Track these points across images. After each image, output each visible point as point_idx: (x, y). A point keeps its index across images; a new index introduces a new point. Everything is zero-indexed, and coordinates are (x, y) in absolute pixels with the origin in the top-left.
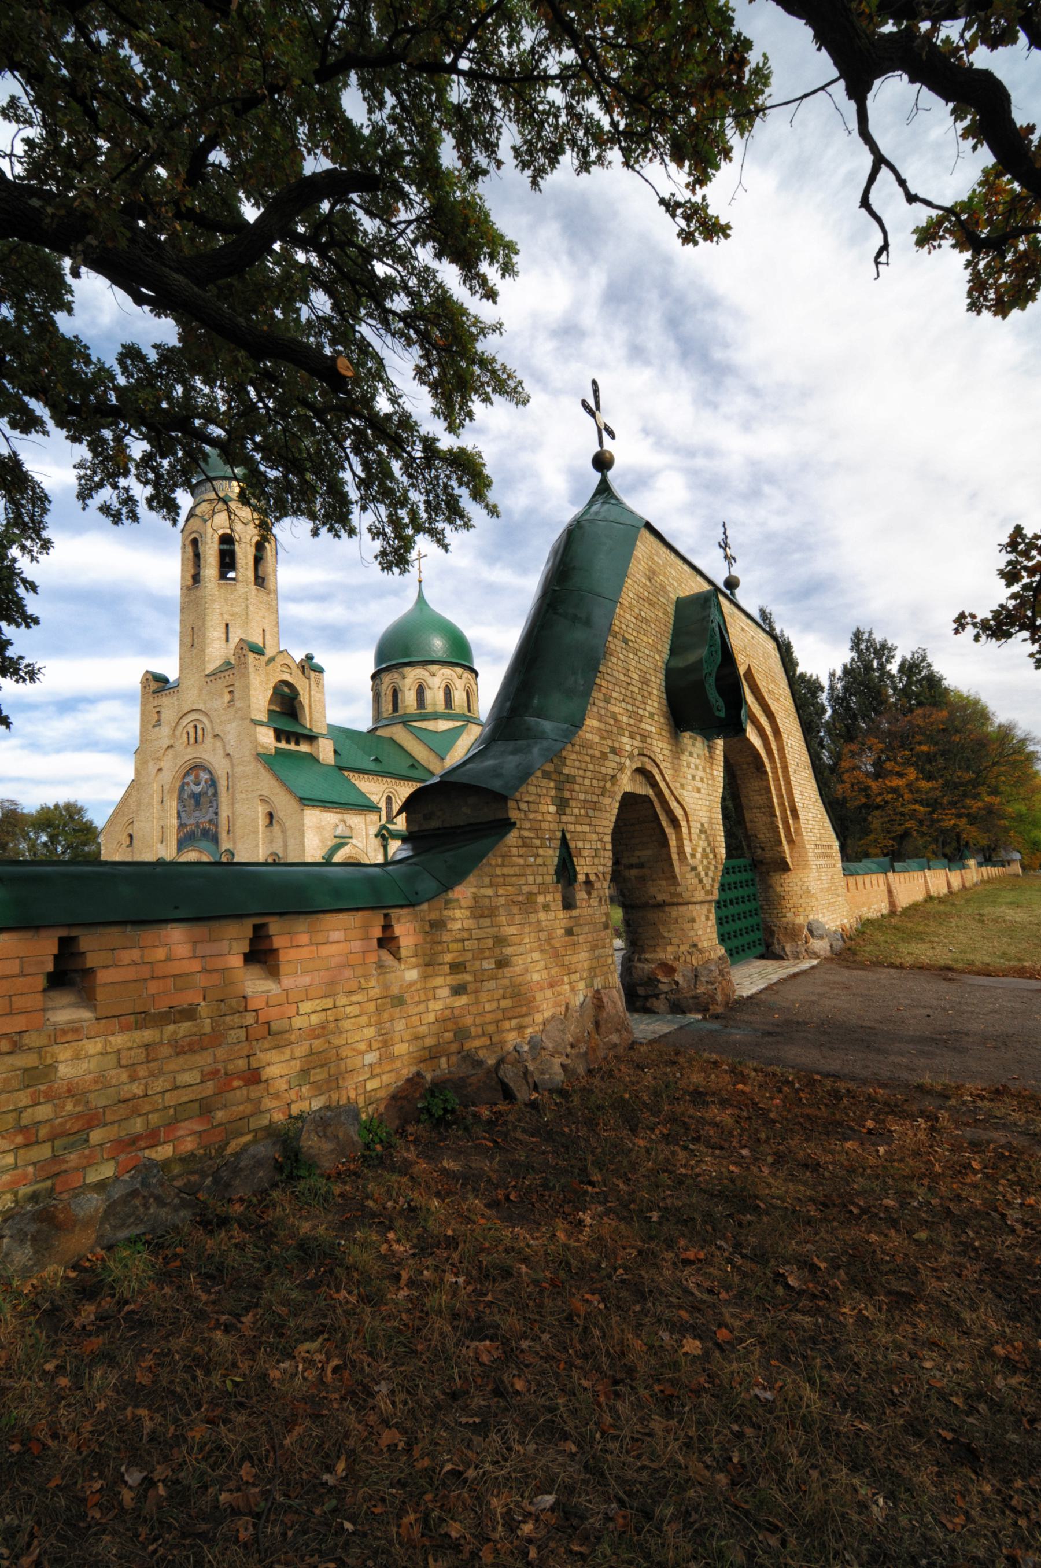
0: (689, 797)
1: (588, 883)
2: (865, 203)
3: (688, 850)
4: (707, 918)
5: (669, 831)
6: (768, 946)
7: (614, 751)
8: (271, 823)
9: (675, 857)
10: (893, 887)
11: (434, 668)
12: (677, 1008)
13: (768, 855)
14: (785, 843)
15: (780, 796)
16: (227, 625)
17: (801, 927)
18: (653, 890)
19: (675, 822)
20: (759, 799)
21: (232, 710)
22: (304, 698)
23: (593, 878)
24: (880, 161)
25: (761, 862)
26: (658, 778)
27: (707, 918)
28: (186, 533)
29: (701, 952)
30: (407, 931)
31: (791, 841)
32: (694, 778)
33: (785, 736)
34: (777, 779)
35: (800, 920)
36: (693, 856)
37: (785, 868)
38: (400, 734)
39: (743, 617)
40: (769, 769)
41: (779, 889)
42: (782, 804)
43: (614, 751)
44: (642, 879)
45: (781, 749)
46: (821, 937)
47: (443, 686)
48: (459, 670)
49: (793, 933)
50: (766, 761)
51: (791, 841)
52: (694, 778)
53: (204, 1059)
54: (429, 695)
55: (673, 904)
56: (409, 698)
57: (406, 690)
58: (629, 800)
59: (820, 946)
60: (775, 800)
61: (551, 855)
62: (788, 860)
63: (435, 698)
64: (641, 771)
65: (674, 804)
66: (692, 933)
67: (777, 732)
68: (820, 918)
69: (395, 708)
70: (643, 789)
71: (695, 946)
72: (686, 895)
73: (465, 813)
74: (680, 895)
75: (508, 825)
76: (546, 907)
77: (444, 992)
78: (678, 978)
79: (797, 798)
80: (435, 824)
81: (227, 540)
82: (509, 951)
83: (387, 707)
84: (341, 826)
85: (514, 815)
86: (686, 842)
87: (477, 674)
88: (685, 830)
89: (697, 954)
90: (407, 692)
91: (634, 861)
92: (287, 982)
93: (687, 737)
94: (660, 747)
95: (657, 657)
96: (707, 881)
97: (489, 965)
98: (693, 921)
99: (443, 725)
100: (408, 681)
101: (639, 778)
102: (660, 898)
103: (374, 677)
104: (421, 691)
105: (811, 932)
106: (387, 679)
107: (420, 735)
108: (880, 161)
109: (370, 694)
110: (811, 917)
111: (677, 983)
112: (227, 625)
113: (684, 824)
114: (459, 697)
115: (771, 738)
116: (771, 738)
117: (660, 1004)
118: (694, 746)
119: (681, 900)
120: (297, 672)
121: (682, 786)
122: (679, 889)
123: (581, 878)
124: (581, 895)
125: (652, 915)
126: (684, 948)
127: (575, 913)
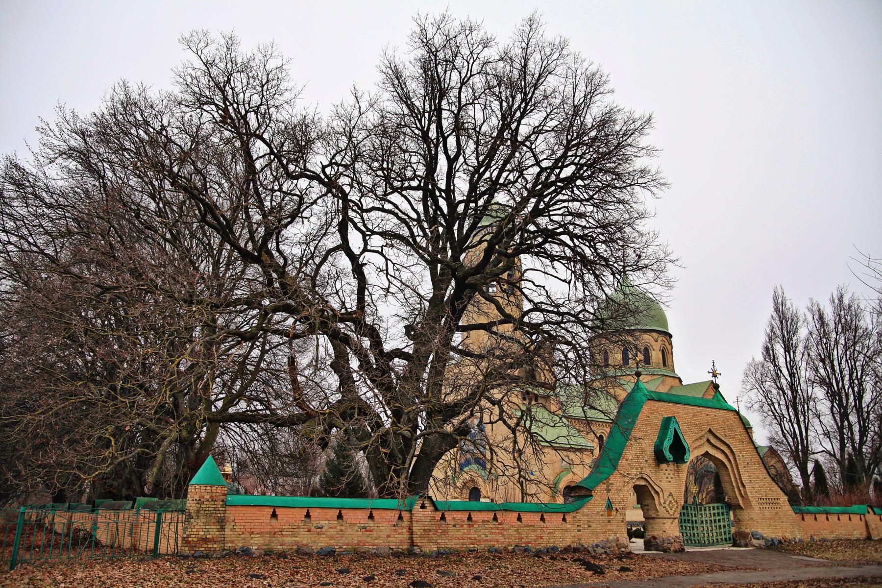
1: (617, 510)
3: (662, 501)
5: (655, 495)
14: (739, 498)
17: (748, 534)
19: (657, 492)
20: (726, 478)
30: (569, 518)
33: (737, 454)
34: (733, 471)
42: (736, 481)
45: (735, 459)
46: (758, 539)
48: (655, 335)
51: (742, 497)
60: (733, 479)
61: (605, 503)
62: (742, 505)
65: (656, 487)
73: (583, 493)
87: (671, 336)
96: (671, 512)
113: (661, 493)
115: (729, 454)
116: (729, 454)
124: (614, 513)
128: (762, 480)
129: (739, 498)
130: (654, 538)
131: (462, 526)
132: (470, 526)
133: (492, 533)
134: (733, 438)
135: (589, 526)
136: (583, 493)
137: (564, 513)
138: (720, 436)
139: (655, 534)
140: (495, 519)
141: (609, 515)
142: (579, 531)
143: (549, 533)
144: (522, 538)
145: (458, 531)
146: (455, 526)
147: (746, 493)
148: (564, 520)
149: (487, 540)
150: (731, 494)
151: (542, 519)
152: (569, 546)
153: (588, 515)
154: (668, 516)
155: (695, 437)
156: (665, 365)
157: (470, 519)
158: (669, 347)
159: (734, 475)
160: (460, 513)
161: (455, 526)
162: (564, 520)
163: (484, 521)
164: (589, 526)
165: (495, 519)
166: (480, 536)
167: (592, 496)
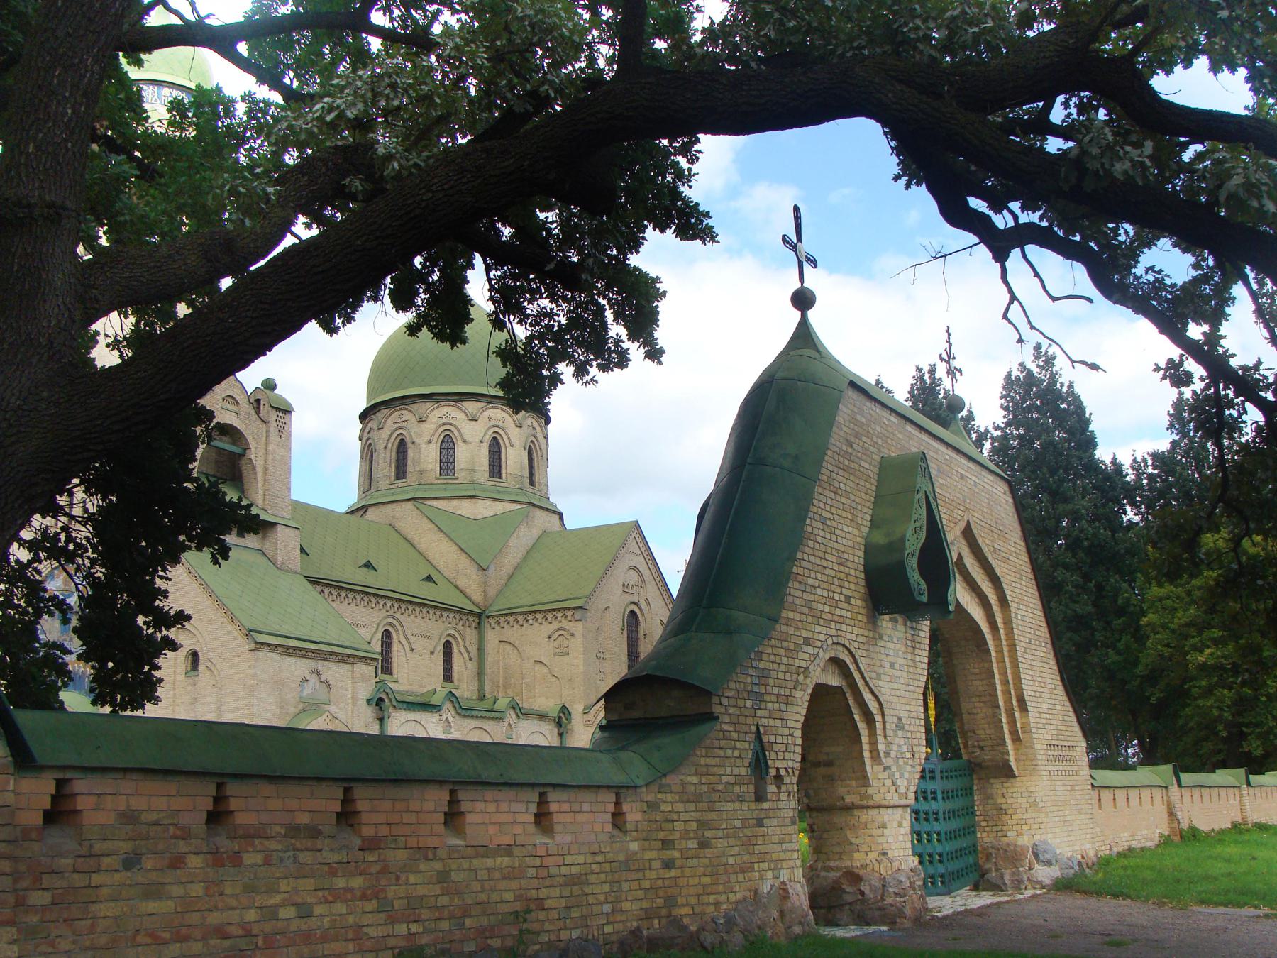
0: (885, 688)
1: (778, 777)
2: (1005, 317)
3: (881, 747)
4: (900, 825)
5: (862, 726)
6: (983, 874)
7: (807, 641)
8: (195, 667)
9: (866, 754)
11: (472, 406)
12: (861, 920)
13: (987, 756)
14: (1009, 742)
15: (1005, 682)
17: (1024, 849)
18: (841, 791)
20: (978, 685)
22: (256, 455)
23: (783, 772)
24: (1013, 298)
25: (979, 765)
26: (852, 668)
27: (900, 825)
29: (890, 861)
31: (1016, 739)
32: (892, 666)
33: (1013, 606)
35: (1024, 841)
36: (887, 754)
37: (1008, 773)
38: (409, 519)
39: (964, 461)
40: (991, 648)
41: (1000, 801)
43: (807, 641)
44: (831, 779)
45: (1008, 622)
46: (1049, 863)
47: (488, 438)
49: (1013, 857)
50: (988, 637)
51: (1016, 739)
52: (892, 666)
53: (514, 885)
54: (462, 455)
55: (863, 807)
56: (426, 456)
57: (422, 442)
58: (820, 691)
59: (1045, 874)
60: (999, 687)
61: (746, 747)
62: (1013, 764)
63: (471, 456)
64: (835, 661)
65: (868, 697)
66: (881, 840)
67: (1003, 601)
68: (1049, 838)
69: (401, 472)
70: (833, 679)
71: (885, 854)
74: (871, 797)
75: (711, 717)
76: (740, 798)
77: (656, 864)
78: (865, 887)
79: (1026, 684)
80: (636, 714)
82: (708, 834)
83: (384, 467)
84: (313, 680)
85: (717, 710)
86: (880, 739)
88: (879, 725)
89: (885, 862)
90: (424, 446)
91: (823, 758)
92: (558, 839)
93: (885, 622)
94: (853, 633)
95: (856, 532)
96: (902, 784)
97: (693, 844)
98: (884, 826)
99: (484, 509)
100: (429, 427)
101: (831, 668)
102: (848, 799)
104: (447, 446)
105: (1036, 855)
106: (390, 421)
107: (447, 528)
108: (1013, 298)
109: (358, 445)
110: (1037, 837)
111: (862, 893)
113: (878, 718)
114: (514, 459)
117: (844, 916)
118: (892, 628)
119: (871, 803)
120: (246, 408)
121: (879, 676)
122: (870, 791)
123: (773, 772)
124: (772, 788)
125: (839, 819)
126: (873, 856)
127: (766, 805)
129: (1007, 736)
130: (854, 877)
131: (177, 862)
132: (217, 860)
133: (337, 896)
135: (704, 844)
136: (669, 704)
137: (619, 790)
139: (858, 860)
140: (347, 816)
141: (760, 797)
142: (668, 864)
143: (571, 881)
144: (466, 912)
145: (153, 892)
146: (131, 862)
147: (1027, 731)
148: (618, 818)
149: (307, 937)
150: (984, 730)
151: (542, 818)
152: (636, 933)
153: (698, 798)
156: (532, 483)
157: (217, 817)
158: (542, 441)
159: (1004, 673)
160: (171, 786)
161: (131, 862)
162: (618, 818)
163: (294, 831)
164: (704, 844)
165: (347, 816)
166: (270, 914)
167: (711, 717)
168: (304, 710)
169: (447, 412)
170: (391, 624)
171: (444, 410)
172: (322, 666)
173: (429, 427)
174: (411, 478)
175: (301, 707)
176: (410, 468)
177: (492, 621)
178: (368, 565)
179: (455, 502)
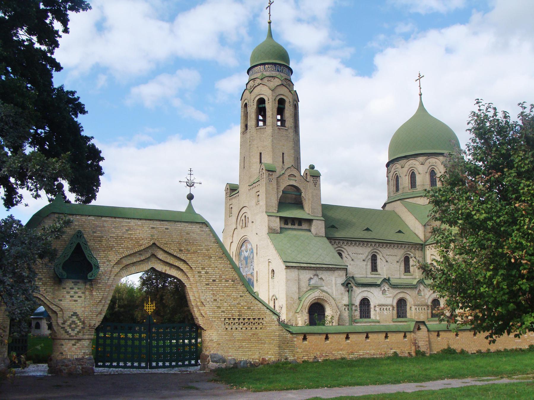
3: (60, 321)
10: (432, 340)
11: (421, 159)
16: (261, 153)
19: (55, 312)
21: (258, 206)
28: (243, 100)
35: (207, 353)
38: (399, 208)
54: (419, 179)
69: (397, 190)
72: (58, 337)
81: (261, 101)
90: (404, 177)
100: (406, 169)
103: (388, 165)
110: (212, 352)
112: (261, 153)
113: (60, 314)
128: (235, 299)
134: (194, 253)
138: (171, 251)
154: (68, 337)
155: (127, 253)
168: (310, 289)
169: (412, 162)
170: (375, 252)
171: (411, 161)
172: (318, 272)
173: (406, 169)
174: (400, 191)
175: (309, 288)
176: (400, 187)
177: (428, 247)
178: (367, 229)
179: (415, 199)
